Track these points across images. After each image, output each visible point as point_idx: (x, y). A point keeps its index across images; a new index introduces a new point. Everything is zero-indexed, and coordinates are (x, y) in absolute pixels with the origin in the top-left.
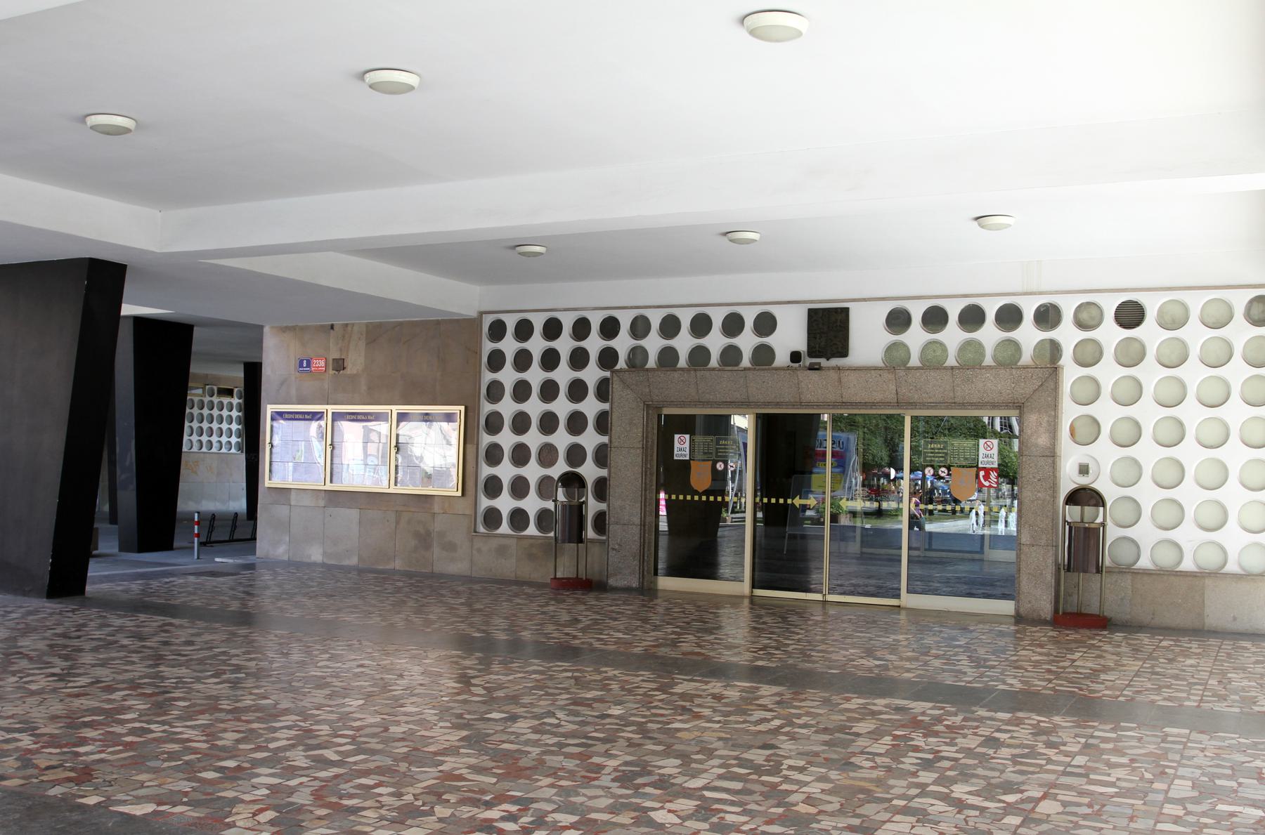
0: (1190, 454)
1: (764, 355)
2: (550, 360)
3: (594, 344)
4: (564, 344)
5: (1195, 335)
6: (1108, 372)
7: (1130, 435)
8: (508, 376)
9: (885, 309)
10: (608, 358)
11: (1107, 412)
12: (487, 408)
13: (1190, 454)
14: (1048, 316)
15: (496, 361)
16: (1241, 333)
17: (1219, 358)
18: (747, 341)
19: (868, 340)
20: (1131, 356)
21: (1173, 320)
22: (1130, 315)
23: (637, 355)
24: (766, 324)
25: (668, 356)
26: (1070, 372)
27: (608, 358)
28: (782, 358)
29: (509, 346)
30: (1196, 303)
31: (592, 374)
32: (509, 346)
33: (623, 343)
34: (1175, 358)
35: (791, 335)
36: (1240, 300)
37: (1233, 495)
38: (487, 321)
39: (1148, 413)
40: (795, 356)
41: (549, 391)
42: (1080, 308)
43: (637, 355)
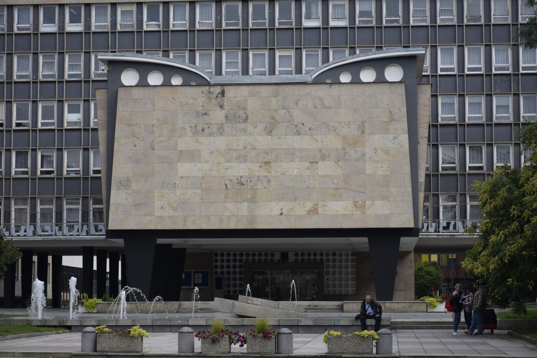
0: (343, 276)
1: (272, 260)
2: (228, 261)
3: (238, 258)
4: (232, 258)
5: (344, 258)
6: (331, 263)
7: (334, 273)
8: (219, 264)
9: (294, 252)
10: (241, 261)
11: (331, 270)
12: (215, 270)
13: (343, 276)
14: (321, 254)
15: (216, 261)
16: (350, 257)
17: (347, 261)
18: (269, 258)
19: (292, 258)
20: (334, 261)
21: (340, 255)
22: (334, 254)
23: (247, 260)
24: (273, 255)
25: (253, 260)
26: (325, 263)
27: (241, 261)
28: (276, 260)
29: (219, 258)
30: (344, 253)
31: (238, 264)
32: (219, 258)
33: (244, 258)
34: (341, 261)
35: (277, 257)
36: (350, 252)
37: (350, 282)
38: (214, 252)
39: (337, 270)
40: (279, 261)
41: (228, 267)
42: (327, 253)
43: (247, 260)
